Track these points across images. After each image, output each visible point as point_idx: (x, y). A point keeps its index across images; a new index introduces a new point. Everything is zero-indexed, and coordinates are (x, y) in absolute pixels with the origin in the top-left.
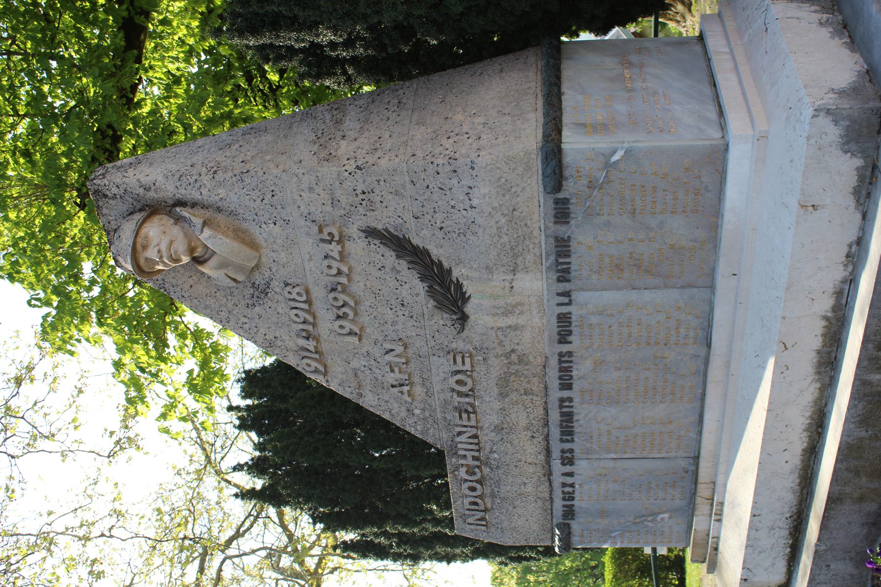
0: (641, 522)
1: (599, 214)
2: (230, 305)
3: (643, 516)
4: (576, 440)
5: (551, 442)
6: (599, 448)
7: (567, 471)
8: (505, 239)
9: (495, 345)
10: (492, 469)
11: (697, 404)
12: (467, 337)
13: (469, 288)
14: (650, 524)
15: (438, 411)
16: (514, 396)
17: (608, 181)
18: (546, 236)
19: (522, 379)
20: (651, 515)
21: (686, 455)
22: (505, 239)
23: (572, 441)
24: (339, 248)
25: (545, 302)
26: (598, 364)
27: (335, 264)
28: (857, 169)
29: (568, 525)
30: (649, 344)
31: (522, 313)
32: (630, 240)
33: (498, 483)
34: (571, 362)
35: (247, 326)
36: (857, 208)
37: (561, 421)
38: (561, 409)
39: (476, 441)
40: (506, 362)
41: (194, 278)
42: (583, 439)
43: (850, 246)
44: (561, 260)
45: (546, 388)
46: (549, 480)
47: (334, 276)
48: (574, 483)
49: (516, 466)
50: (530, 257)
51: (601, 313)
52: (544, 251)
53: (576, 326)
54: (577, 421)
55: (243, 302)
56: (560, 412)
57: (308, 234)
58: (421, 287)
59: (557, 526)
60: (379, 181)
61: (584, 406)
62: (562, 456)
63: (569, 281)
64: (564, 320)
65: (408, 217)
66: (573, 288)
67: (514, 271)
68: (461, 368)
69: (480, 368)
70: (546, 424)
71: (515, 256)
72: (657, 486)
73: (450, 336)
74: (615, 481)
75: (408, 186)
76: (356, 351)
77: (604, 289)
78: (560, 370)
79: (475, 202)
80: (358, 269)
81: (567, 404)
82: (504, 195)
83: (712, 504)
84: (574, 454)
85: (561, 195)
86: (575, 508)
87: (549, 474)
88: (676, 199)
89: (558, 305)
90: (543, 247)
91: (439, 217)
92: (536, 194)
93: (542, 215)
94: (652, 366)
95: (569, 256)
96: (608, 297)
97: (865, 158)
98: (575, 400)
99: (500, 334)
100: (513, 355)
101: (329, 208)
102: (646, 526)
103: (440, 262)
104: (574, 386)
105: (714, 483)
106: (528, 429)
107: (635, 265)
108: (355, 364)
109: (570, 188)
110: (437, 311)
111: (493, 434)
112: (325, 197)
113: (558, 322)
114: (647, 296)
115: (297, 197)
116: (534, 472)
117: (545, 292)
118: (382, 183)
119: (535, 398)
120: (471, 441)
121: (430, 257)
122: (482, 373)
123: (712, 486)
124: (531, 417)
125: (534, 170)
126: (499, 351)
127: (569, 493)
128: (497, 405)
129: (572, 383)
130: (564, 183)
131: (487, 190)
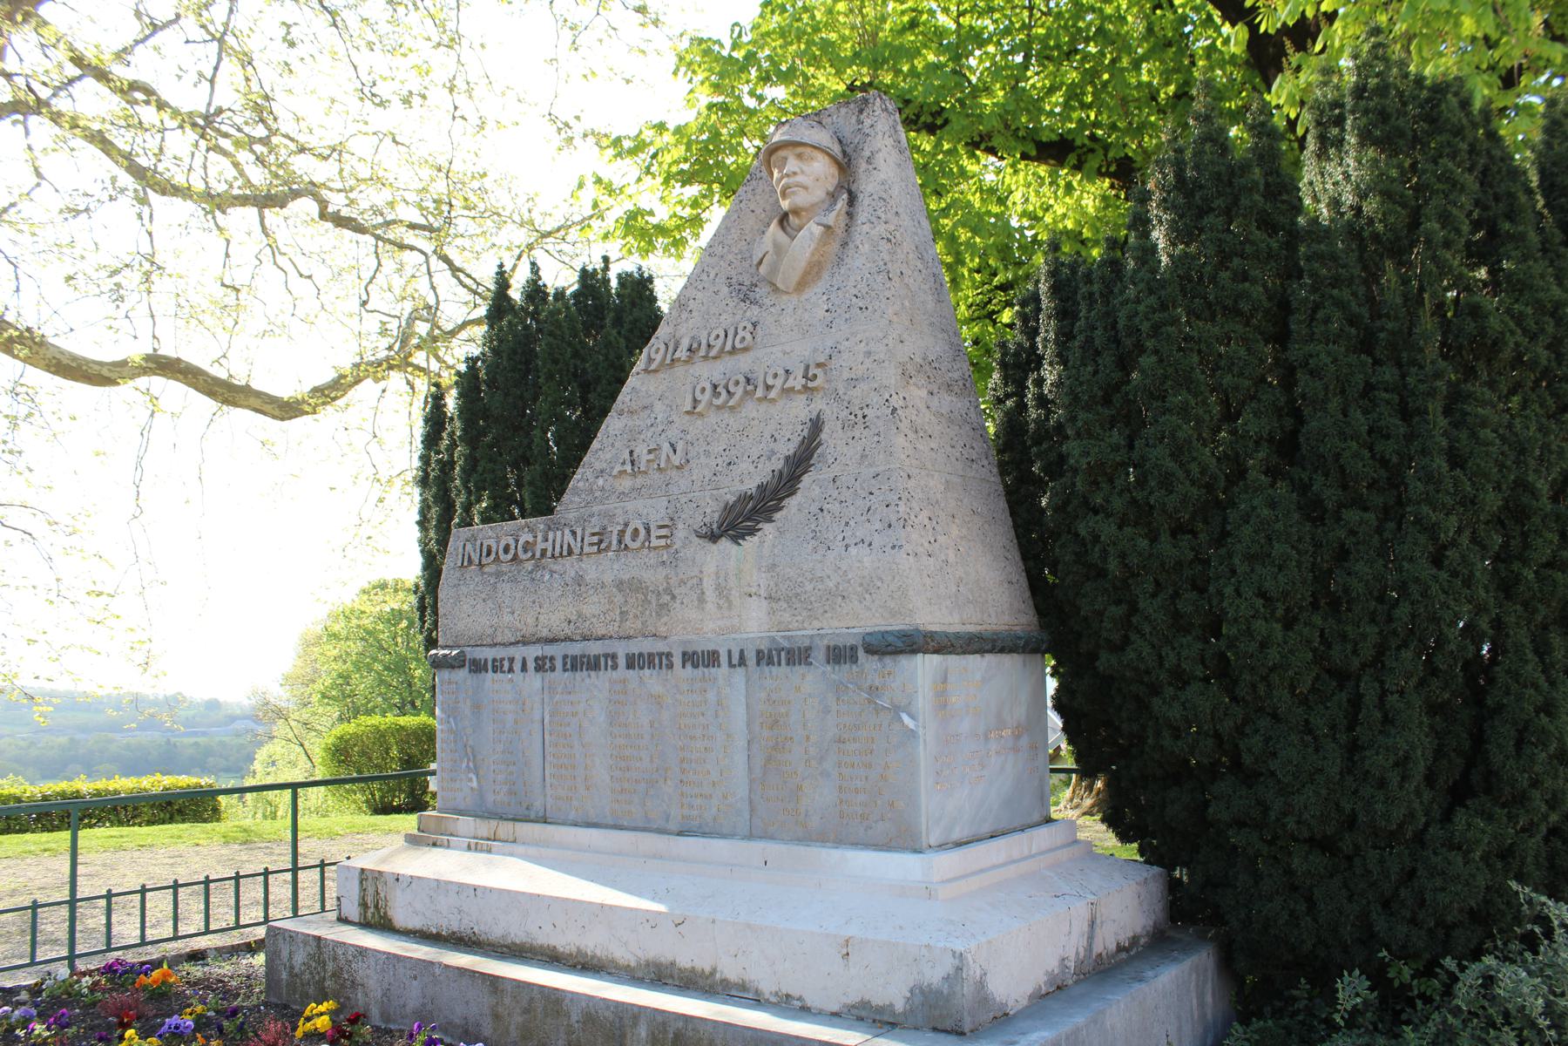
1: (838, 699)
2: (730, 257)
3: (474, 757)
8: (809, 587)
9: (681, 576)
10: (531, 572)
11: (610, 821)
13: (750, 543)
14: (464, 765)
15: (601, 507)
16: (619, 599)
17: (878, 710)
20: (475, 766)
21: (548, 807)
23: (565, 670)
24: (798, 387)
25: (733, 636)
26: (658, 700)
27: (778, 382)
28: (891, 1005)
29: (463, 666)
30: (682, 761)
31: (719, 607)
32: (808, 738)
33: (514, 580)
35: (704, 277)
36: (845, 1005)
39: (565, 553)
40: (661, 589)
43: (800, 999)
44: (783, 654)
45: (629, 638)
46: (518, 642)
47: (765, 382)
50: (787, 617)
51: (719, 703)
55: (733, 273)
57: (815, 350)
58: (751, 486)
59: (462, 652)
63: (758, 664)
64: (711, 659)
65: (836, 470)
67: (769, 598)
68: (654, 533)
69: (652, 558)
70: (585, 638)
71: (788, 600)
72: (511, 773)
73: (690, 521)
74: (516, 722)
75: (873, 471)
78: (650, 655)
79: (853, 550)
82: (861, 585)
83: (489, 839)
85: (861, 653)
86: (483, 673)
87: (525, 642)
88: (857, 791)
89: (730, 652)
90: (799, 633)
91: (835, 508)
92: (862, 623)
93: (837, 631)
95: (788, 664)
96: (739, 712)
97: (904, 1013)
100: (669, 598)
101: (846, 375)
103: (781, 509)
105: (514, 841)
107: (777, 743)
109: (869, 664)
110: (722, 505)
111: (573, 574)
112: (860, 371)
114: (740, 759)
115: (859, 337)
116: (526, 622)
117: (745, 636)
118: (876, 438)
119: (617, 624)
120: (565, 547)
121: (788, 496)
123: (511, 839)
124: (594, 620)
127: (502, 666)
128: (608, 578)
130: (876, 657)
131: (867, 565)
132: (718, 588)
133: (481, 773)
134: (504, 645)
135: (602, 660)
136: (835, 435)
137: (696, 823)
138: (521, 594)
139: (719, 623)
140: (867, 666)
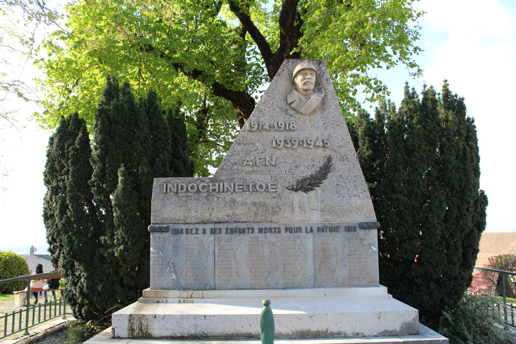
0: (169, 266)
1: (349, 242)
2: (277, 99)
4: (228, 235)
5: (225, 224)
6: (222, 245)
7: (207, 231)
8: (337, 208)
9: (283, 202)
10: (207, 197)
11: (249, 287)
12: (285, 191)
13: (312, 193)
14: (168, 270)
16: (254, 209)
17: (363, 245)
18: (339, 223)
19: (264, 212)
20: (175, 271)
21: (217, 284)
22: (337, 208)
23: (227, 233)
24: (321, 146)
25: (307, 222)
26: (274, 244)
27: (313, 143)
28: (395, 330)
29: (168, 231)
30: (284, 264)
31: (301, 213)
32: (337, 255)
33: (197, 199)
34: (275, 233)
36: (379, 333)
37: (240, 229)
38: (247, 228)
40: (274, 206)
41: (285, 88)
42: (228, 238)
43: (362, 333)
44: (328, 229)
45: (259, 222)
46: (200, 223)
47: (307, 142)
48: (198, 234)
49: (209, 208)
50: (329, 217)
52: (332, 222)
53: (295, 235)
54: (240, 235)
56: (245, 228)
57: (322, 135)
58: (308, 174)
60: (353, 164)
61: (249, 238)
62: (217, 229)
63: (318, 232)
64: (299, 229)
65: (340, 173)
66: (314, 233)
71: (329, 212)
72: (196, 272)
73: (284, 184)
74: (199, 253)
75: (354, 175)
76: (265, 145)
77: (314, 246)
78: (270, 228)
80: (310, 151)
81: (250, 231)
82: (357, 208)
83: (187, 298)
84: (218, 234)
85: (357, 229)
86: (180, 235)
87: (204, 223)
88: (356, 270)
89: (306, 228)
92: (357, 220)
93: (349, 222)
94: (272, 266)
95: (330, 232)
96: (310, 247)
97: (400, 332)
98: (252, 235)
99: (290, 204)
100: (278, 209)
101: (337, 145)
102: (166, 268)
103: (322, 183)
104: (261, 234)
105: (203, 298)
106: (234, 214)
107: (325, 257)
108: (257, 144)
109: (361, 233)
111: (229, 199)
112: (342, 144)
113: (297, 228)
114: (310, 263)
115: (338, 134)
116: (206, 216)
117: (312, 223)
118: (353, 165)
122: (266, 196)
123: (201, 296)
125: (367, 219)
126: (280, 203)
127: (191, 232)
128: (249, 201)
129: (262, 233)
130: (363, 230)
132: (300, 207)
133: (178, 273)
134: (192, 223)
135: (247, 230)
136: (337, 162)
137: (291, 284)
138: (202, 205)
139: (300, 218)
140: (360, 232)
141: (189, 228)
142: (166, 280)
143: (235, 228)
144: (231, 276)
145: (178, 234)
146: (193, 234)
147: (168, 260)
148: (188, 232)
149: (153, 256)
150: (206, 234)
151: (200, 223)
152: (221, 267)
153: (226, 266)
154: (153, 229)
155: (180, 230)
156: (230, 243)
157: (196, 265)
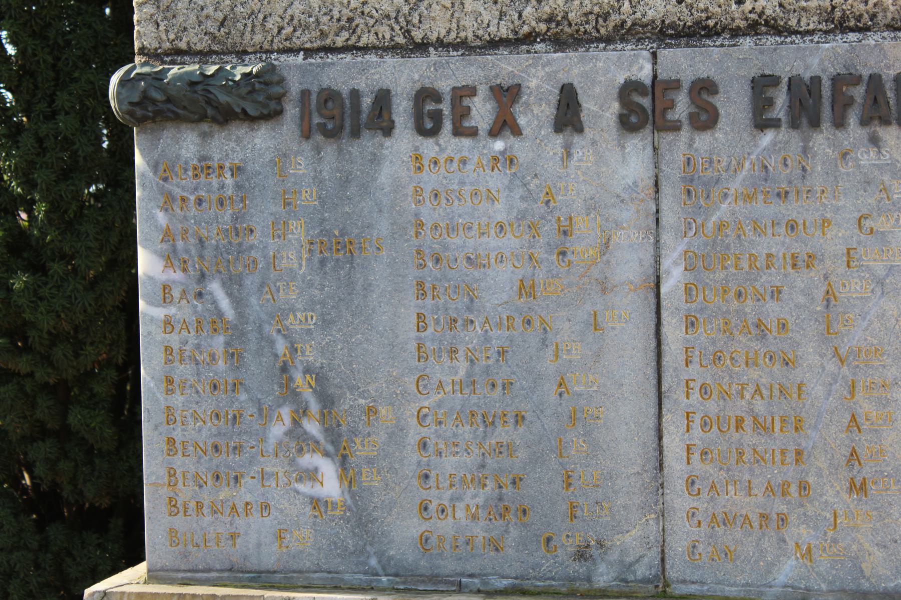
0: (291, 395)
4: (768, 138)
5: (747, 42)
6: (721, 226)
7: (588, 105)
14: (277, 431)
20: (333, 433)
21: (678, 546)
23: (762, 123)
37: (875, 81)
42: (773, 162)
46: (530, 38)
48: (517, 131)
54: (875, 141)
62: (676, 85)
72: (508, 449)
74: (526, 289)
84: (685, 134)
86: (369, 142)
102: (265, 415)
127: (461, 113)
133: (360, 451)
134: (463, 46)
141: (445, 86)
142: (266, 507)
143: (836, 80)
144: (804, 487)
145: (356, 134)
146: (473, 133)
147: (281, 346)
148: (437, 117)
149: (159, 313)
150: (579, 129)
151: (530, 38)
152: (712, 407)
153: (760, 406)
154: (145, 99)
155: (367, 102)
156: (791, 210)
157: (507, 386)
